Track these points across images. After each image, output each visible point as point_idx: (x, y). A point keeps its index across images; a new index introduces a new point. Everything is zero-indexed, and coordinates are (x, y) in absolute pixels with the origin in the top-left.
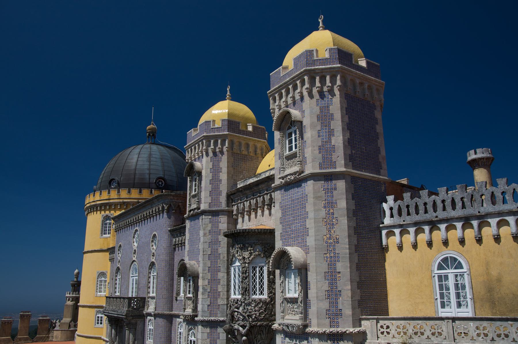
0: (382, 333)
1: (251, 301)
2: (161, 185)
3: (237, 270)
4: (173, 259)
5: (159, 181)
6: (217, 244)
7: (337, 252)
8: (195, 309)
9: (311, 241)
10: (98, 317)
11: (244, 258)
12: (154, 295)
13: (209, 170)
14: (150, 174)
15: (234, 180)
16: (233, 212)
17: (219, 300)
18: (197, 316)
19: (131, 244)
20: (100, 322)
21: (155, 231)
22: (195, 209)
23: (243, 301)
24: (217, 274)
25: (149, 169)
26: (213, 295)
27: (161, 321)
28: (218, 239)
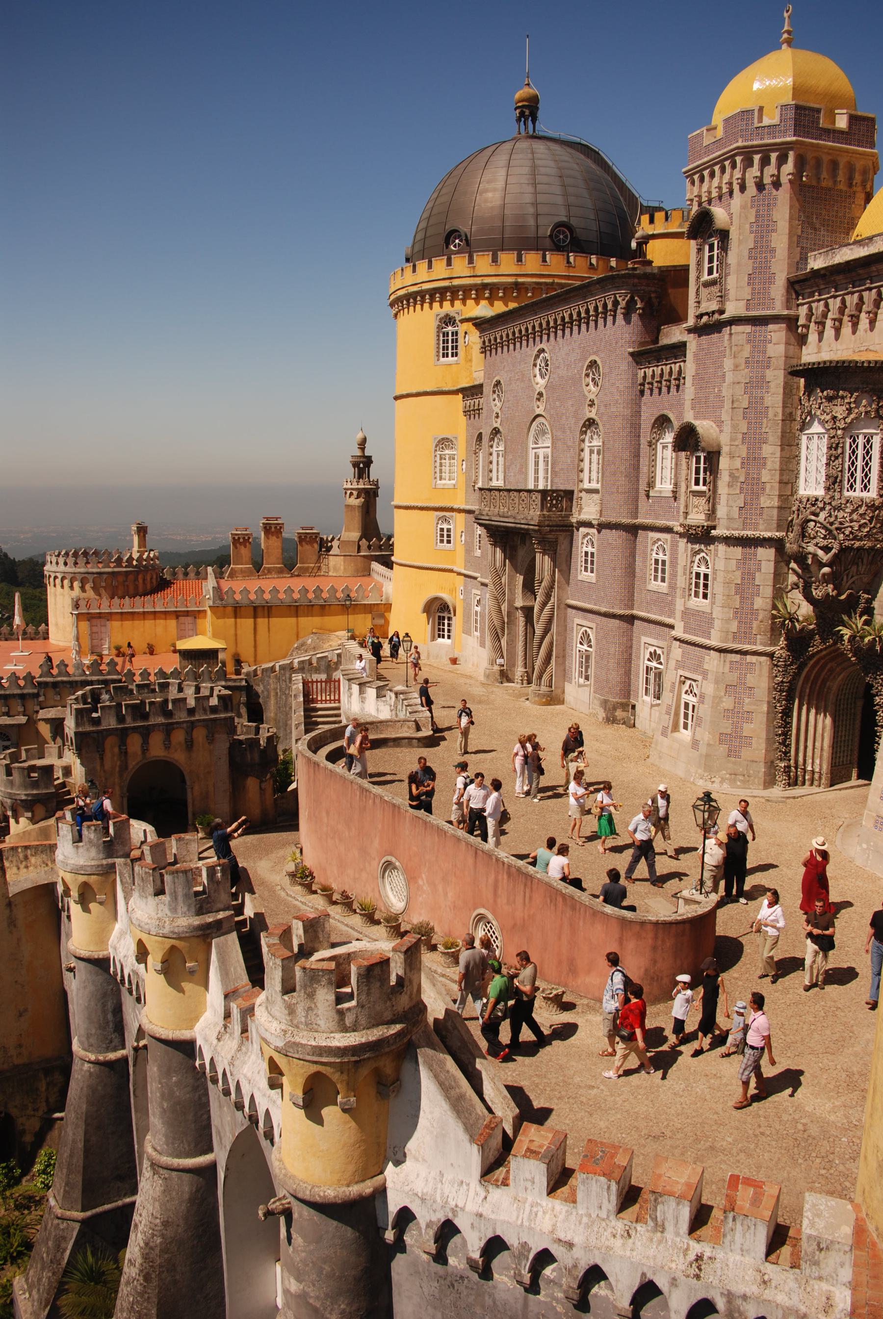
2: (564, 241)
4: (637, 413)
5: (559, 232)
6: (761, 387)
8: (712, 514)
10: (442, 530)
11: (834, 418)
12: (594, 485)
13: (748, 226)
14: (537, 215)
17: (762, 499)
18: (714, 528)
20: (445, 539)
22: (713, 312)
23: (827, 501)
25: (535, 204)
26: (752, 488)
28: (764, 377)
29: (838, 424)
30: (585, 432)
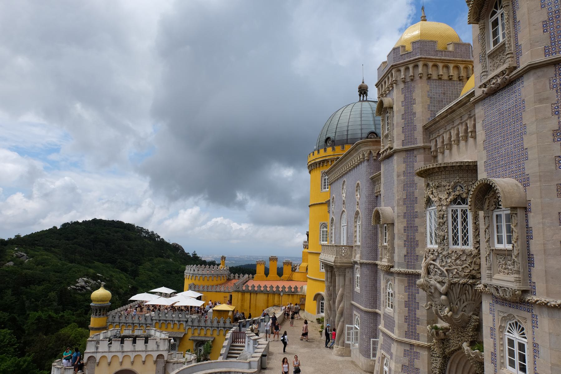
1: (450, 252)
3: (433, 214)
8: (391, 259)
9: (531, 167)
15: (432, 111)
16: (431, 148)
18: (393, 267)
21: (359, 180)
23: (440, 251)
27: (366, 270)
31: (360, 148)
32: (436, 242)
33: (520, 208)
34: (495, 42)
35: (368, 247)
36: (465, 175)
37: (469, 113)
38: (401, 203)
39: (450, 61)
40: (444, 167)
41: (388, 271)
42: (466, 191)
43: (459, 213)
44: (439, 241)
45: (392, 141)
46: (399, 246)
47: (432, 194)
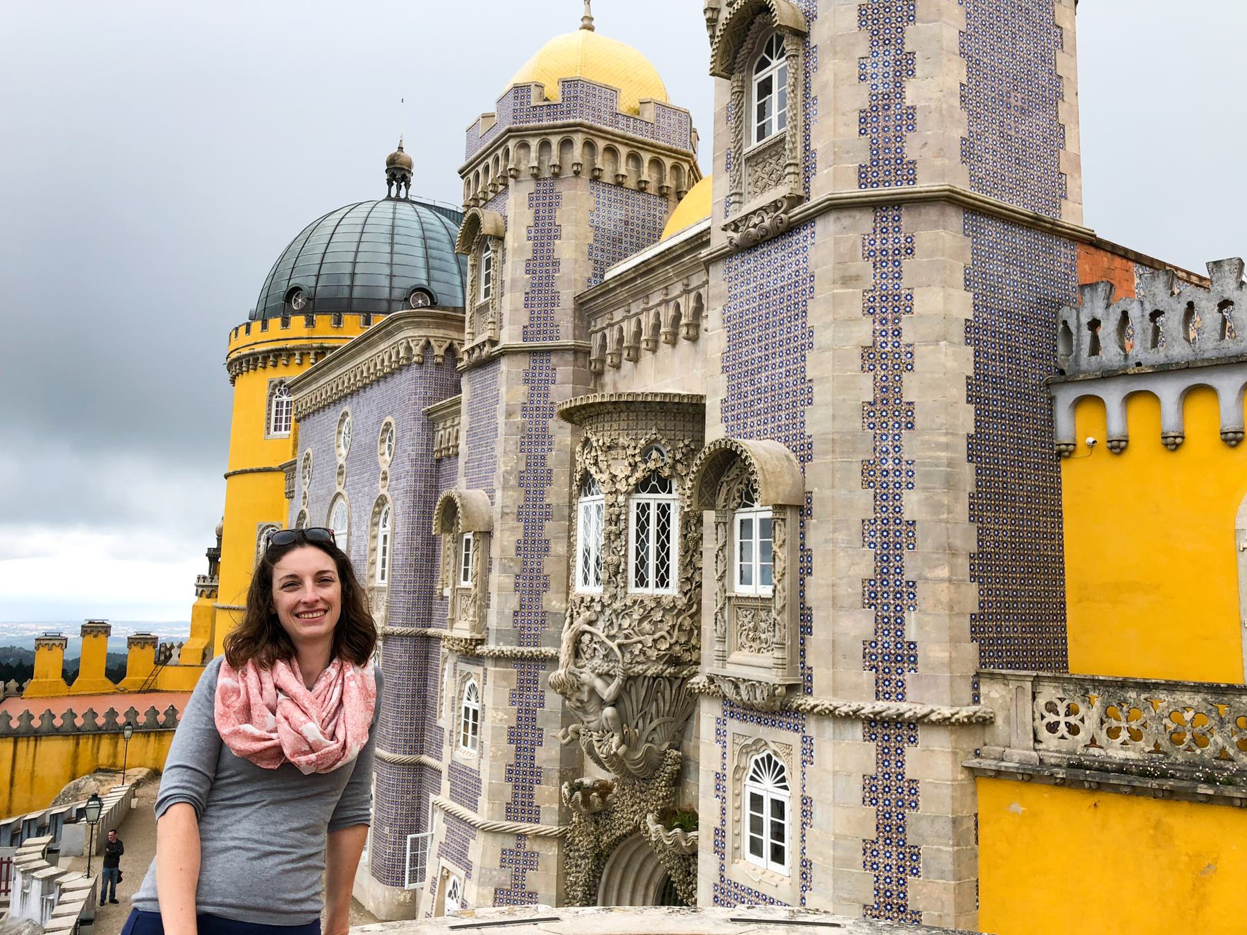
0: (1053, 728)
1: (629, 603)
3: (593, 511)
4: (435, 489)
6: (543, 443)
7: (906, 457)
8: (481, 623)
9: (817, 422)
12: (384, 583)
16: (589, 353)
18: (481, 642)
19: (330, 450)
21: (390, 413)
23: (606, 601)
24: (541, 527)
25: (391, 264)
26: (531, 583)
29: (618, 486)
30: (380, 513)
31: (400, 329)
32: (598, 579)
33: (791, 506)
34: (761, 133)
35: (409, 592)
36: (671, 425)
37: (685, 281)
38: (513, 481)
39: (645, 146)
40: (626, 402)
41: (470, 653)
42: (670, 461)
43: (653, 513)
44: (603, 576)
45: (498, 324)
46: (501, 589)
47: (596, 464)
